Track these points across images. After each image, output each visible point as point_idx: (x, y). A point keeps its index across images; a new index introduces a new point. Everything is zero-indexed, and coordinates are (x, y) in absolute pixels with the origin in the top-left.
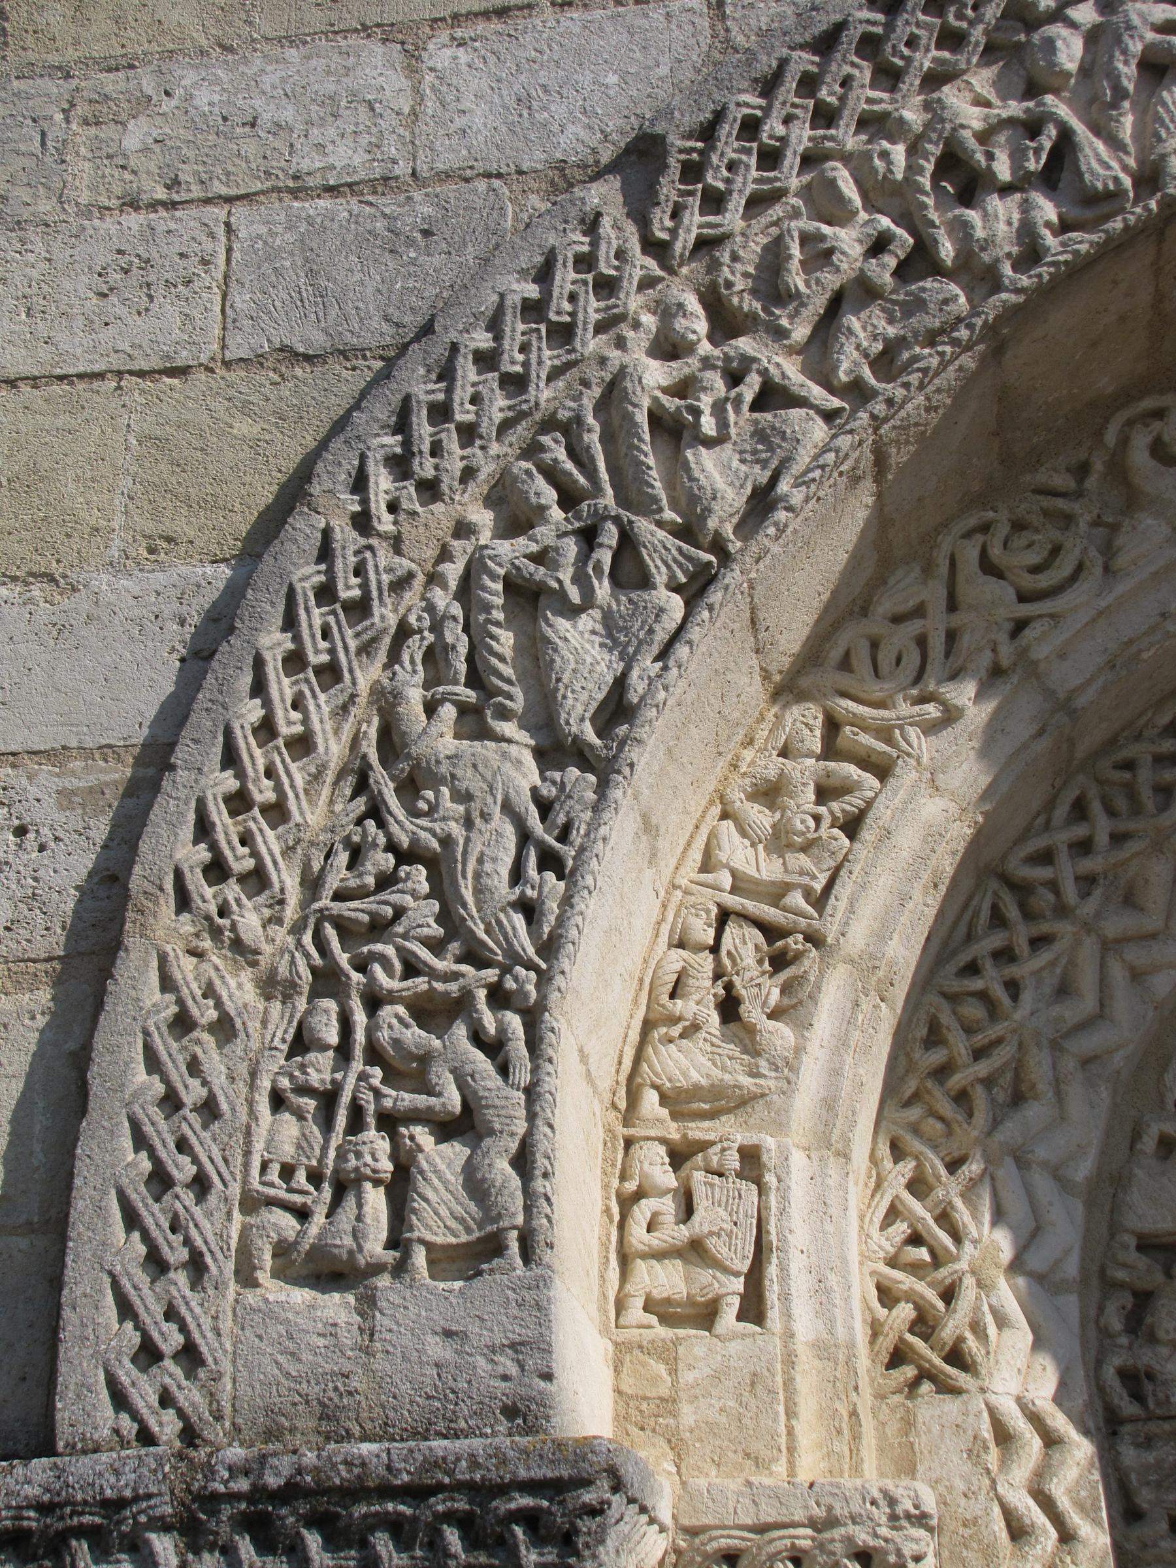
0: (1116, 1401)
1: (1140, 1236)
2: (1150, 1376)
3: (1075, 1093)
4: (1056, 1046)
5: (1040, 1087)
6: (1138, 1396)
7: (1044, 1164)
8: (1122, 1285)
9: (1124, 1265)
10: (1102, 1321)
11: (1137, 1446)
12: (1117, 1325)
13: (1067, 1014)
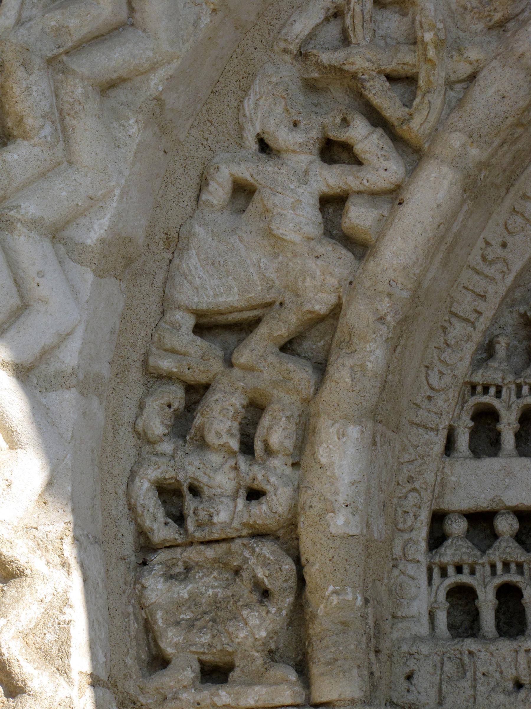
0: (148, 523)
1: (198, 314)
2: (195, 491)
3: (86, 130)
4: (55, 64)
5: (29, 121)
6: (180, 519)
7: (34, 224)
8: (167, 378)
9: (173, 351)
10: (140, 424)
11: (170, 577)
12: (157, 425)
13: (73, 23)
